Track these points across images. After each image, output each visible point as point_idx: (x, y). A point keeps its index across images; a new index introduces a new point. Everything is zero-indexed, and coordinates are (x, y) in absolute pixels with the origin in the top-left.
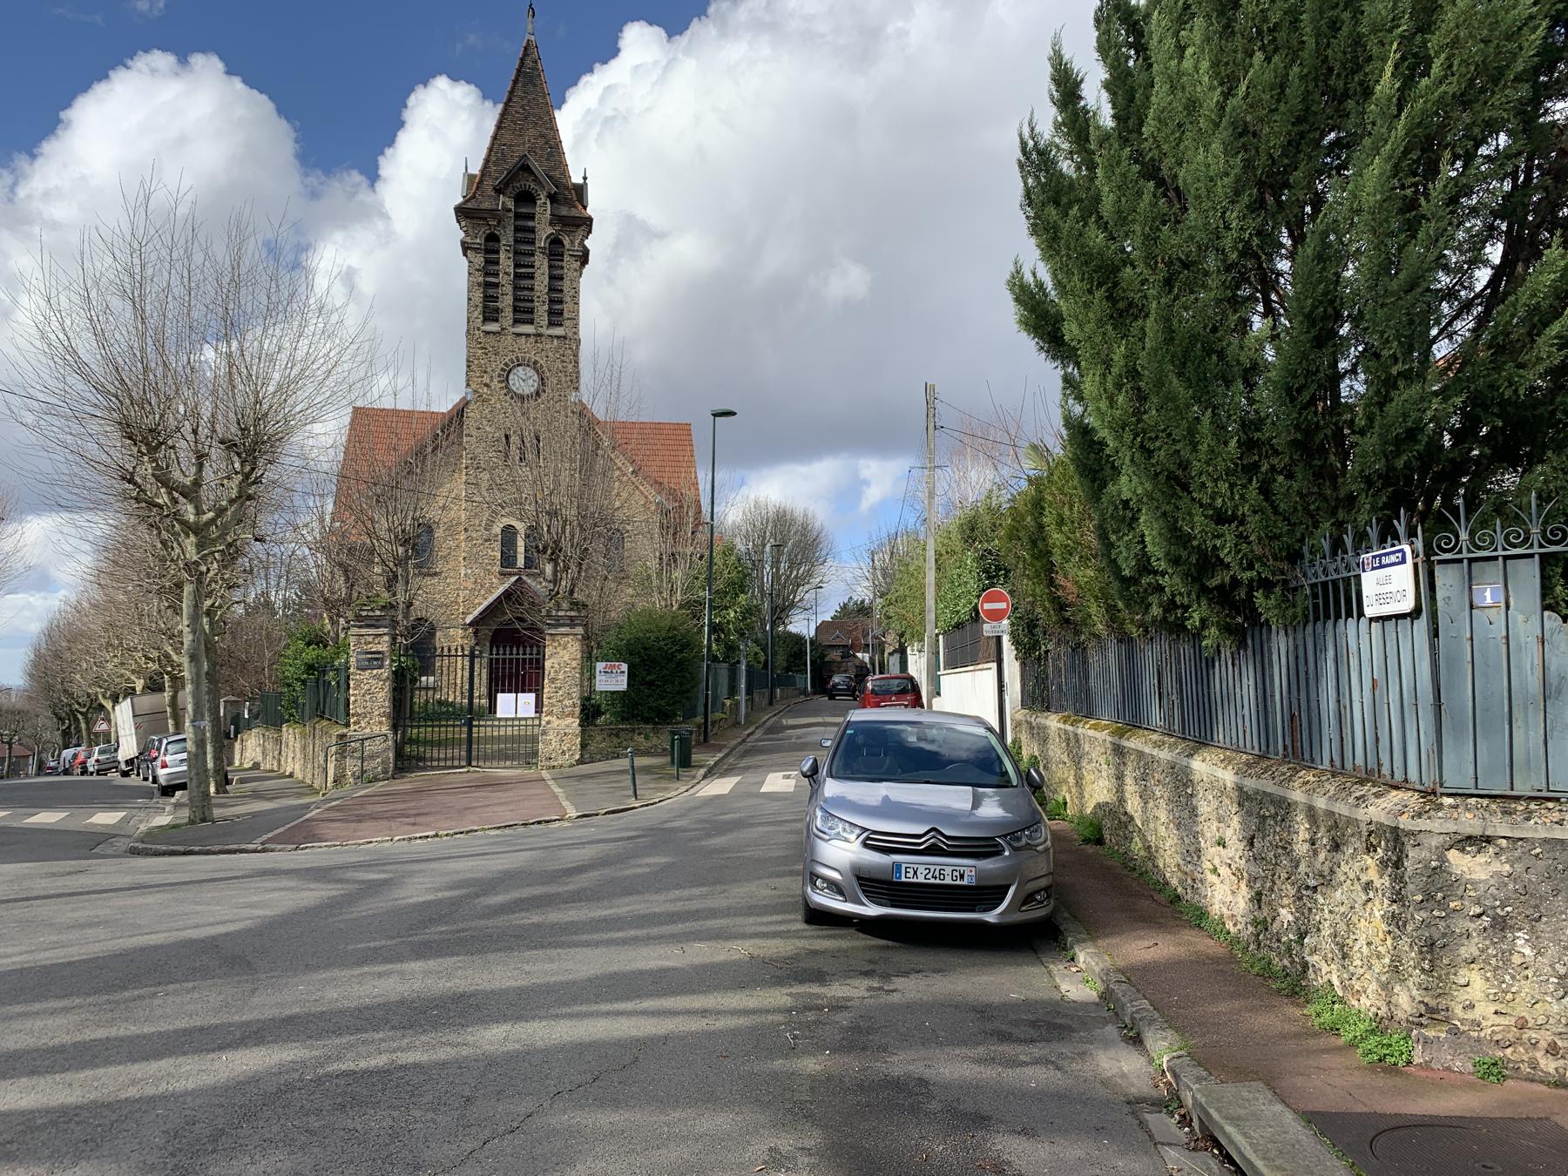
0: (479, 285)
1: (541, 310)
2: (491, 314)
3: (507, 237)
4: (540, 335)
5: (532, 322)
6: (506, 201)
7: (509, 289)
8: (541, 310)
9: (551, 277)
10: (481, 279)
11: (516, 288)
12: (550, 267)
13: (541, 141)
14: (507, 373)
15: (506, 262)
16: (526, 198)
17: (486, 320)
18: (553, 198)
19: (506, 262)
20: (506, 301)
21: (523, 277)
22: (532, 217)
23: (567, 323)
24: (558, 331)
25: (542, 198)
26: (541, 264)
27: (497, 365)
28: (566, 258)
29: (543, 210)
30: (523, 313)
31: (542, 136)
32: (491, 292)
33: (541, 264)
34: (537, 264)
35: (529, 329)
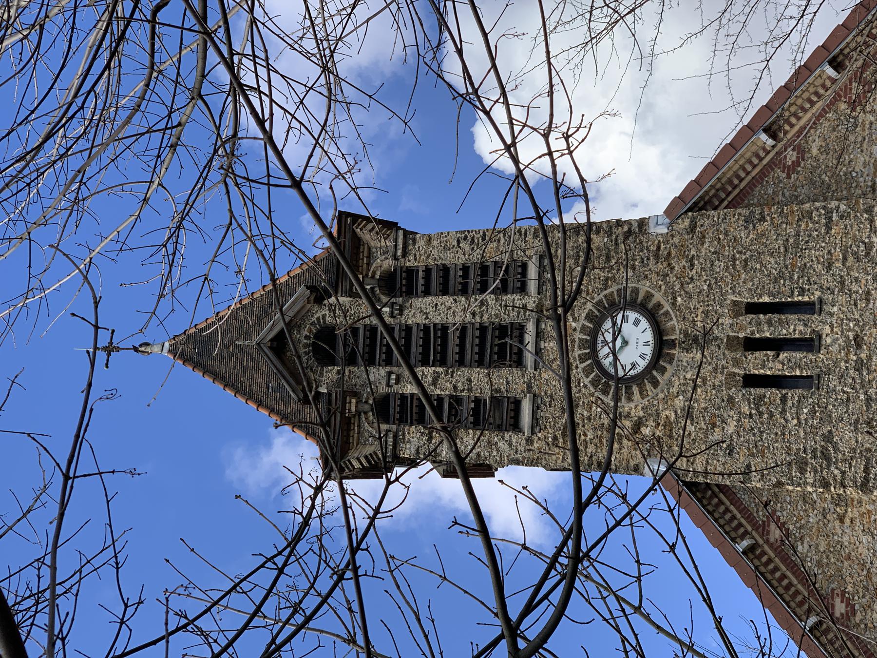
1: (494, 308)
6: (328, 378)
7: (461, 374)
8: (494, 308)
9: (445, 291)
11: (461, 363)
12: (427, 293)
16: (325, 345)
17: (516, 426)
18: (319, 296)
20: (478, 381)
21: (436, 347)
25: (322, 313)
26: (424, 310)
28: (410, 262)
29: (347, 310)
32: (466, 409)
33: (424, 310)
34: (420, 319)
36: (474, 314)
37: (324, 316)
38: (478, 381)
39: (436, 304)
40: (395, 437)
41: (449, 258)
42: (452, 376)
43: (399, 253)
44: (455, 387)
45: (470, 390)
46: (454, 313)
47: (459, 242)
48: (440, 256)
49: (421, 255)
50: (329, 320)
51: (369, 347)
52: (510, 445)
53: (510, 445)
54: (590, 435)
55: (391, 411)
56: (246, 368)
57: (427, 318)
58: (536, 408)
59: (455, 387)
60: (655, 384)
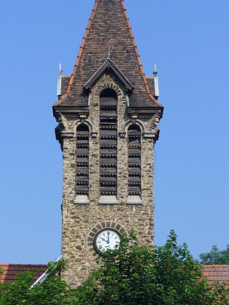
0: (72, 166)
1: (123, 183)
2: (82, 186)
3: (95, 126)
4: (122, 204)
5: (115, 194)
6: (94, 98)
10: (74, 162)
12: (129, 148)
13: (120, 47)
14: (95, 235)
15: (94, 147)
19: (94, 147)
20: (94, 178)
22: (114, 108)
23: (144, 193)
24: (135, 199)
26: (123, 146)
27: (86, 232)
30: (109, 186)
31: (121, 43)
33: (123, 146)
34: (119, 147)
35: (112, 199)
36: (120, 173)
37: (121, 94)
38: (94, 178)
39: (124, 154)
40: (72, 137)
41: (143, 159)
42: (96, 164)
43: (146, 136)
44: (91, 166)
45: (91, 173)
46: (121, 163)
47: (149, 164)
48: (144, 154)
49: (144, 145)
50: (119, 97)
51: (108, 123)
52: (71, 193)
53: (71, 193)
54: (75, 228)
55: (81, 133)
56: (99, 36)
57: (119, 150)
58: (85, 204)
59: (91, 166)
60: (94, 255)
